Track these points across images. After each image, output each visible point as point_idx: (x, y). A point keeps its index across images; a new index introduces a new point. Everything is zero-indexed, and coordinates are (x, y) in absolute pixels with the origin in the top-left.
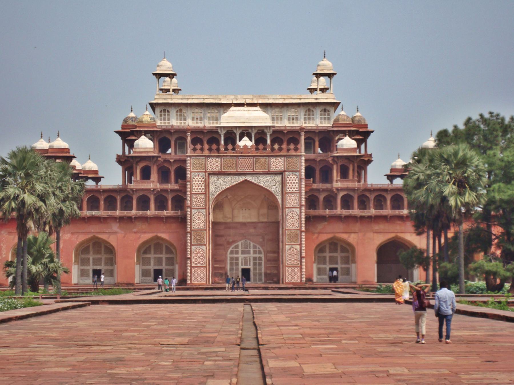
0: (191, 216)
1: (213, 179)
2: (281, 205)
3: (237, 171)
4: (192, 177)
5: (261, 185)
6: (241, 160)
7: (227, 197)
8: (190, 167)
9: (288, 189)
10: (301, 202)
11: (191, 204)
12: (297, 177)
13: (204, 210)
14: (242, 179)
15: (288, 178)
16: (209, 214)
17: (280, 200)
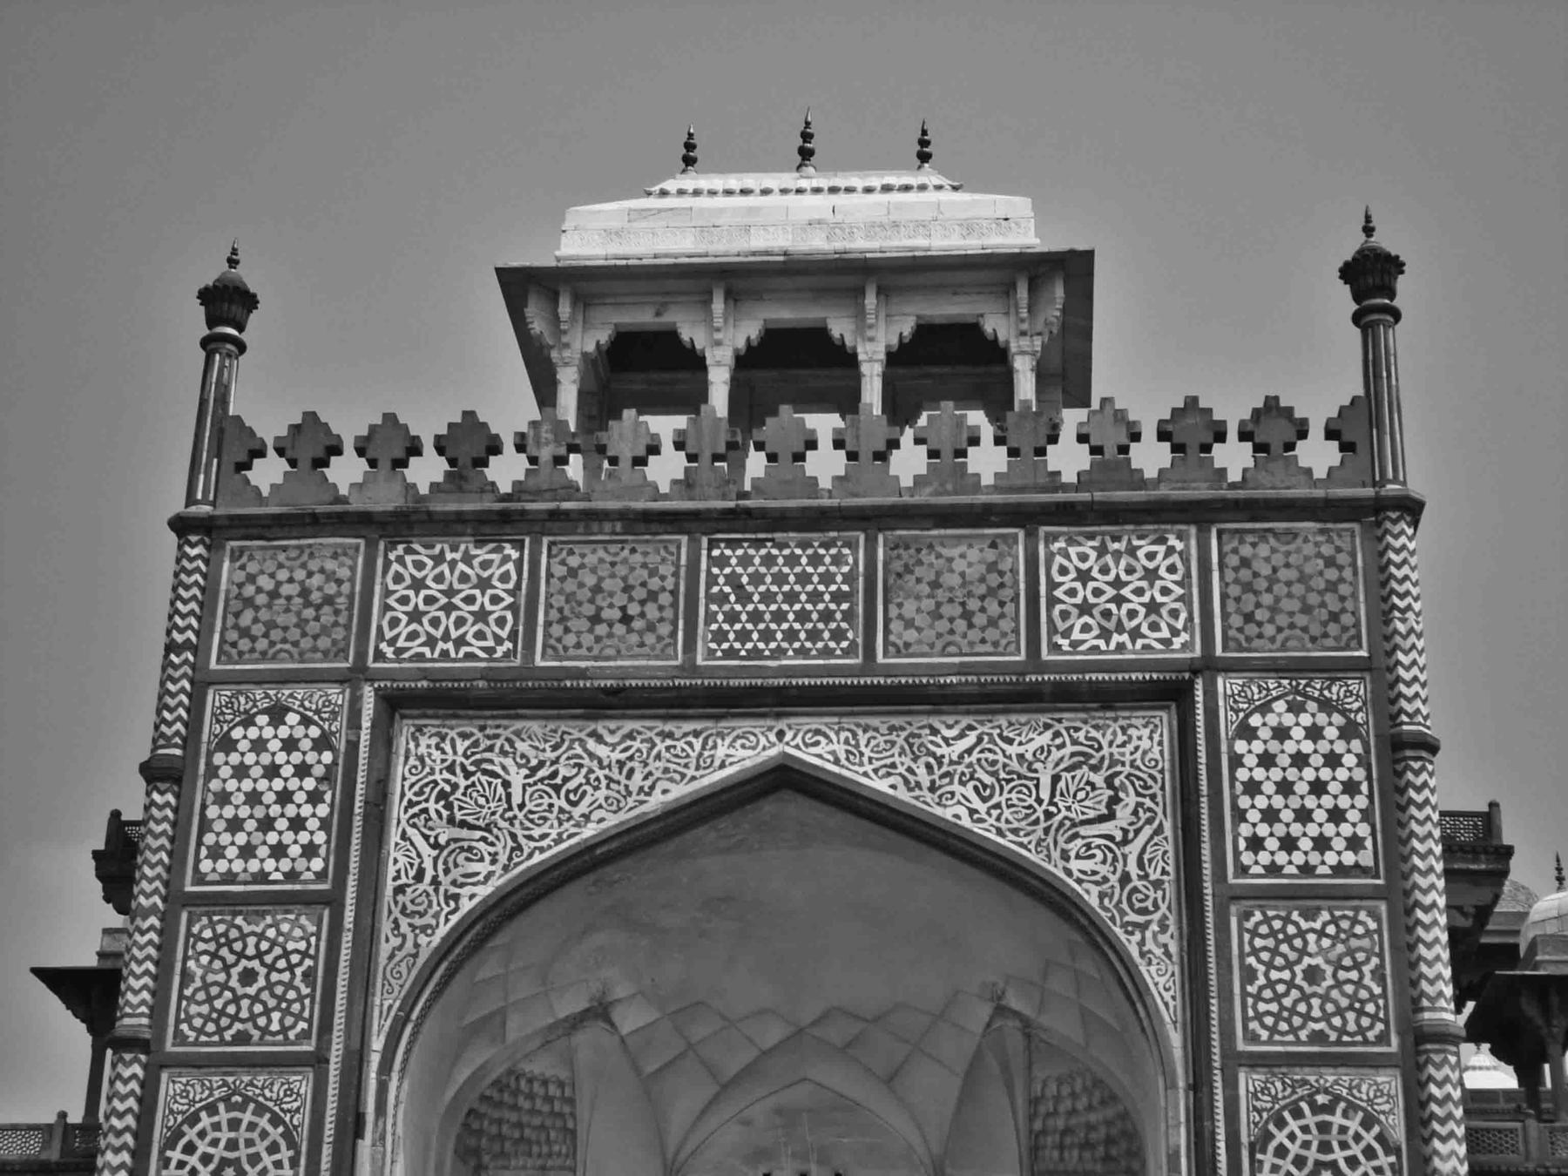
0: (140, 1154)
1: (427, 753)
2: (1175, 1039)
3: (690, 668)
4: (209, 729)
5: (948, 814)
6: (738, 559)
7: (600, 1011)
8: (204, 633)
9: (1255, 848)
10: (1411, 999)
11: (158, 1011)
12: (1348, 732)
13: (303, 1084)
14: (741, 749)
15: (1248, 733)
16: (352, 1126)
17: (1162, 980)
